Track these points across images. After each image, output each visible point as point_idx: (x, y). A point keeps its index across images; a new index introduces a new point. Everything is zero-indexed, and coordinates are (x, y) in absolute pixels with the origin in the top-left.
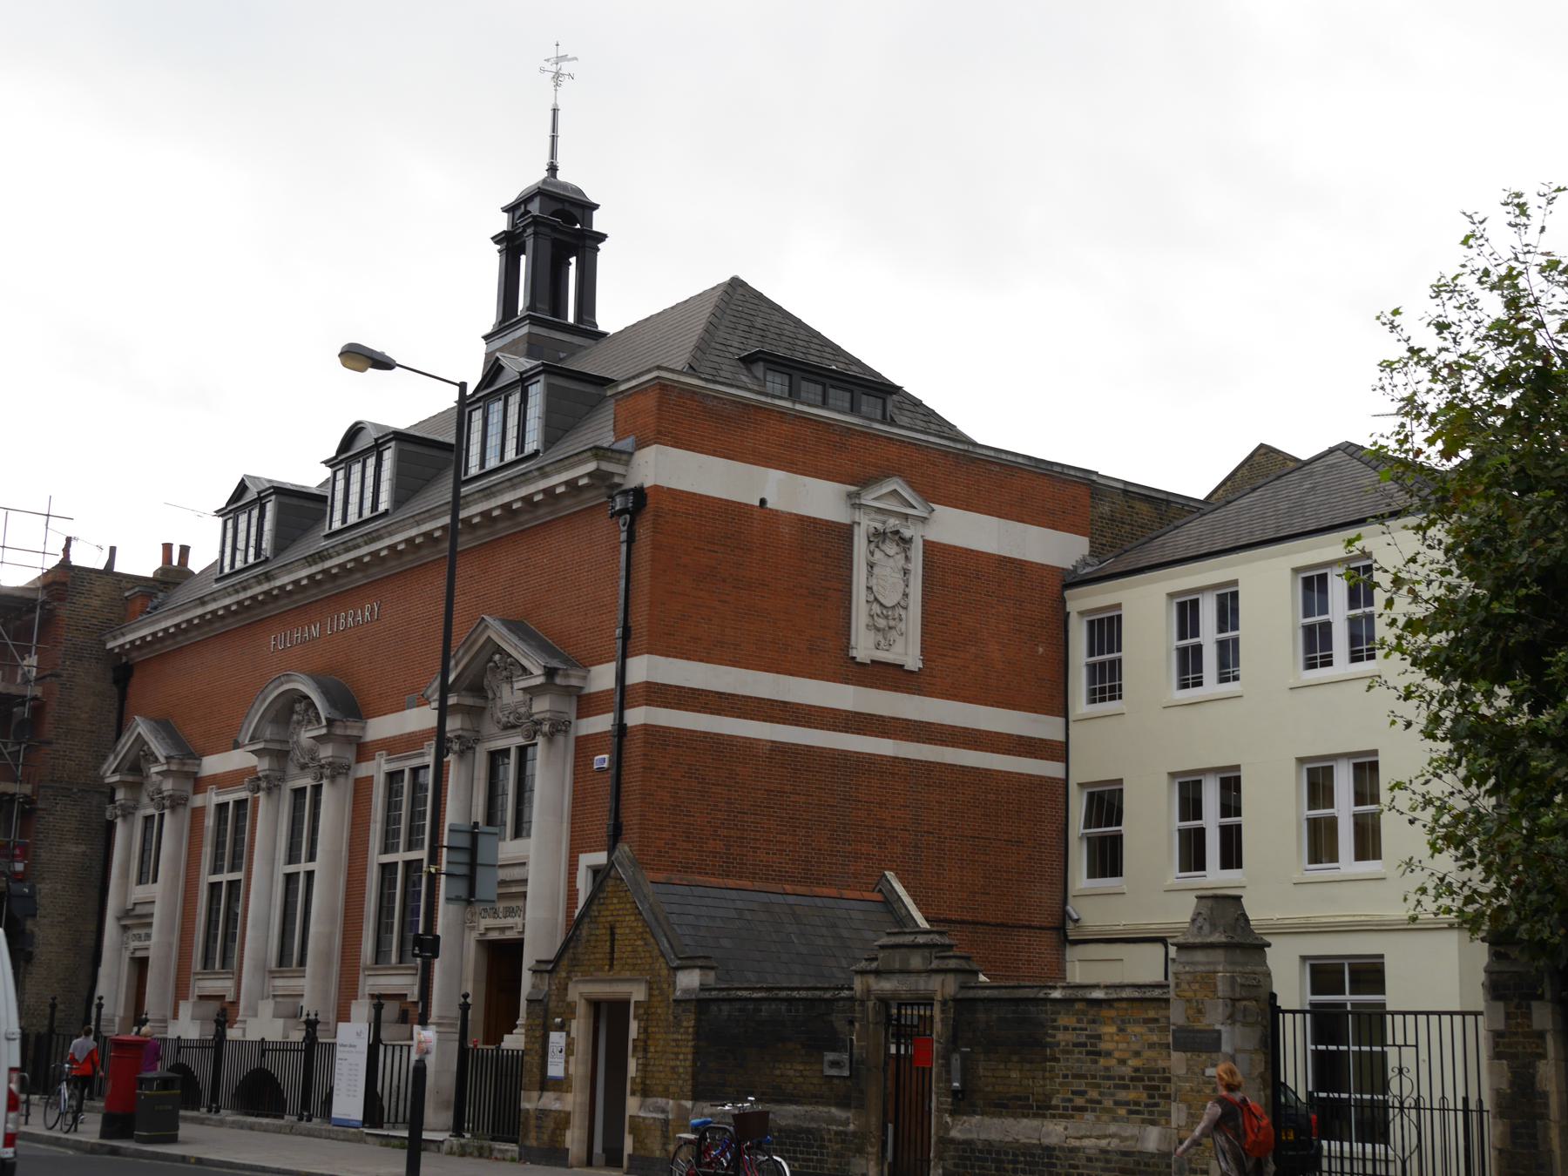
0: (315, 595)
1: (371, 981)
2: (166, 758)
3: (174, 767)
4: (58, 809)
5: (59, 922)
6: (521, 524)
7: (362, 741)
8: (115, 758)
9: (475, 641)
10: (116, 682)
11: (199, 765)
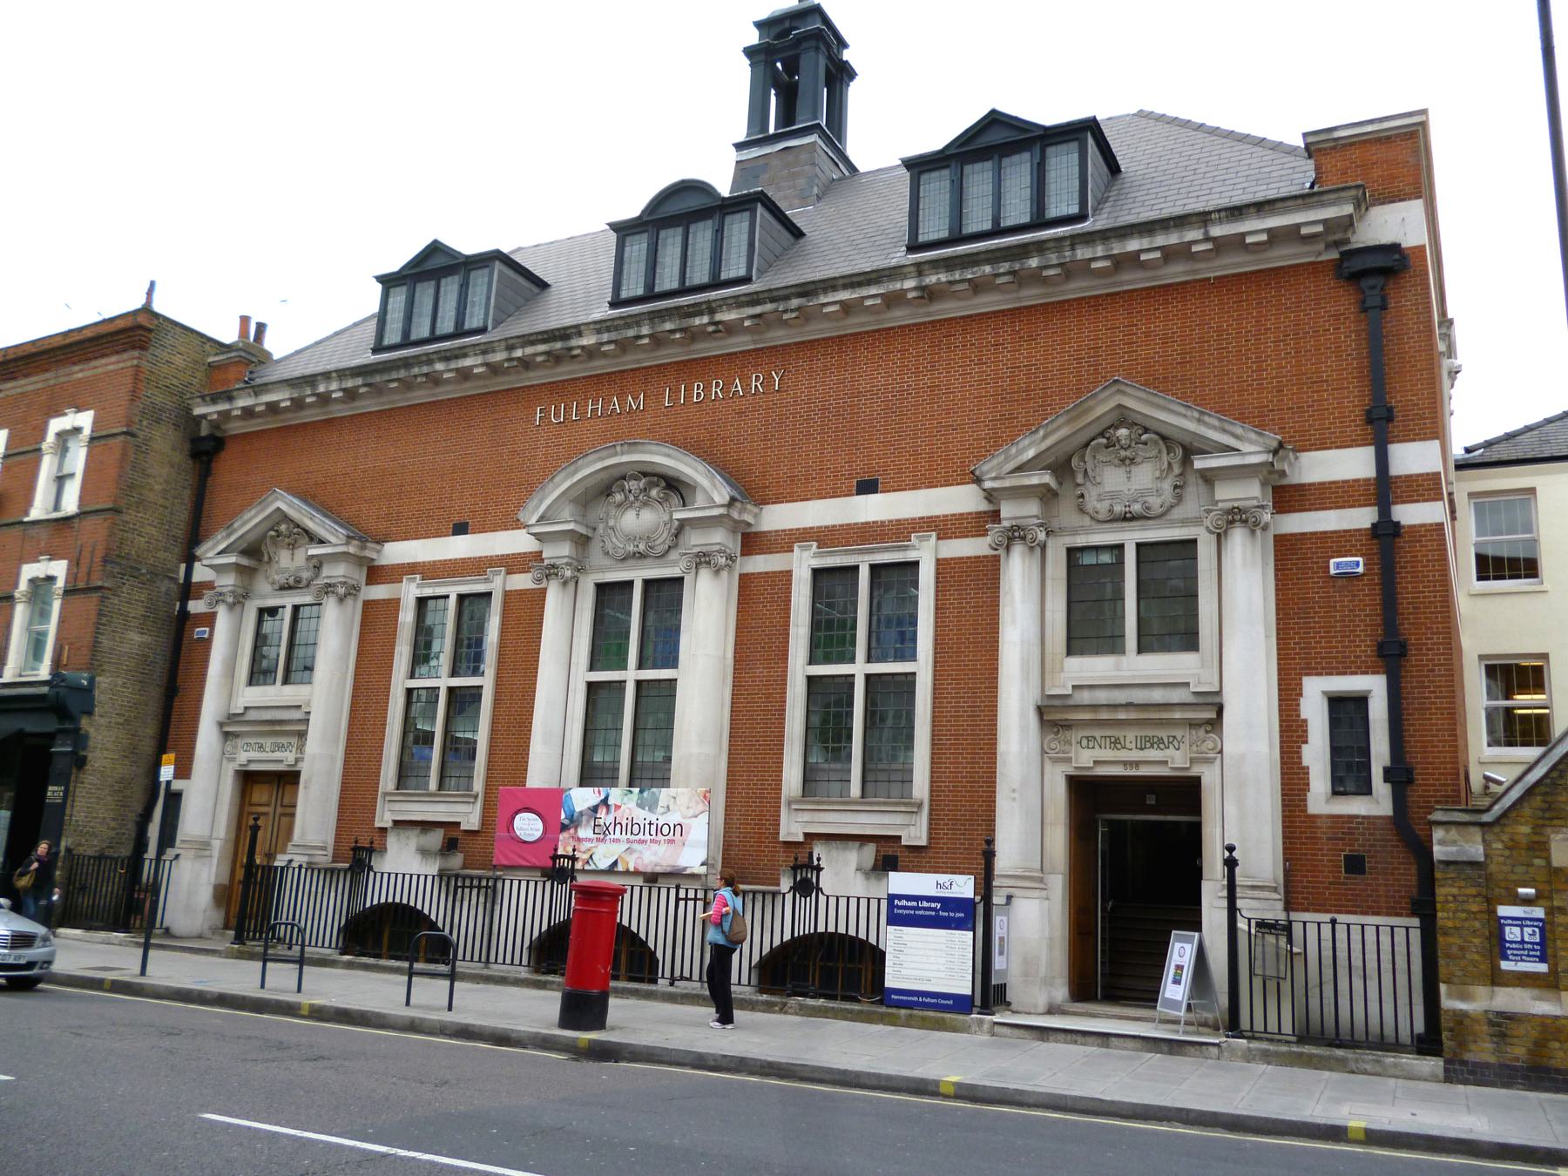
0: (638, 361)
1: (806, 817)
2: (348, 537)
3: (351, 550)
4: (125, 590)
5: (118, 724)
6: (1121, 283)
8: (229, 535)
9: (1090, 409)
10: (196, 455)
11: (379, 552)
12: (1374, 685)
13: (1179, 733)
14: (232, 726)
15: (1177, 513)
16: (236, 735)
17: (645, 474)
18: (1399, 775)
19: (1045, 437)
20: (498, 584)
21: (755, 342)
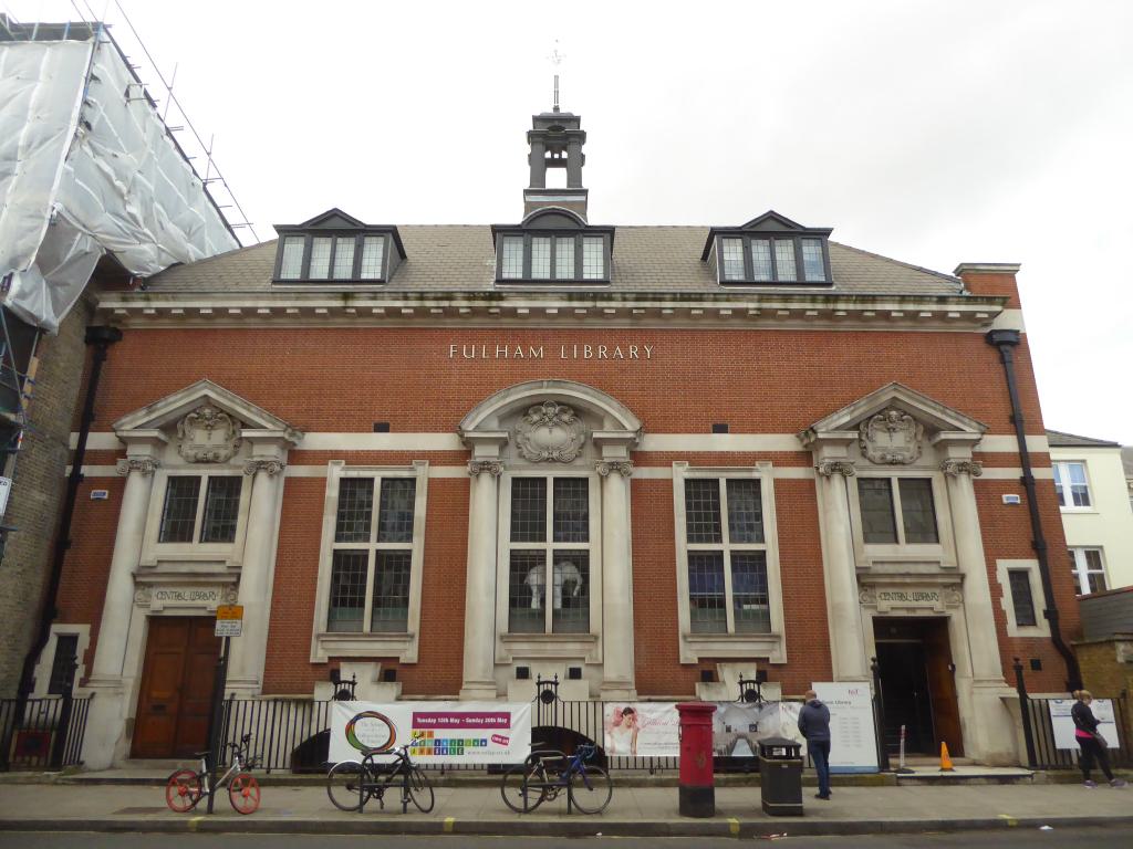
0: (539, 324)
1: (698, 646)
5: (18, 573)
7: (638, 449)
12: (1032, 565)
13: (937, 591)
14: (143, 578)
15: (919, 462)
16: (150, 585)
17: (559, 404)
18: (1050, 614)
19: (853, 411)
20: (423, 473)
21: (632, 324)
